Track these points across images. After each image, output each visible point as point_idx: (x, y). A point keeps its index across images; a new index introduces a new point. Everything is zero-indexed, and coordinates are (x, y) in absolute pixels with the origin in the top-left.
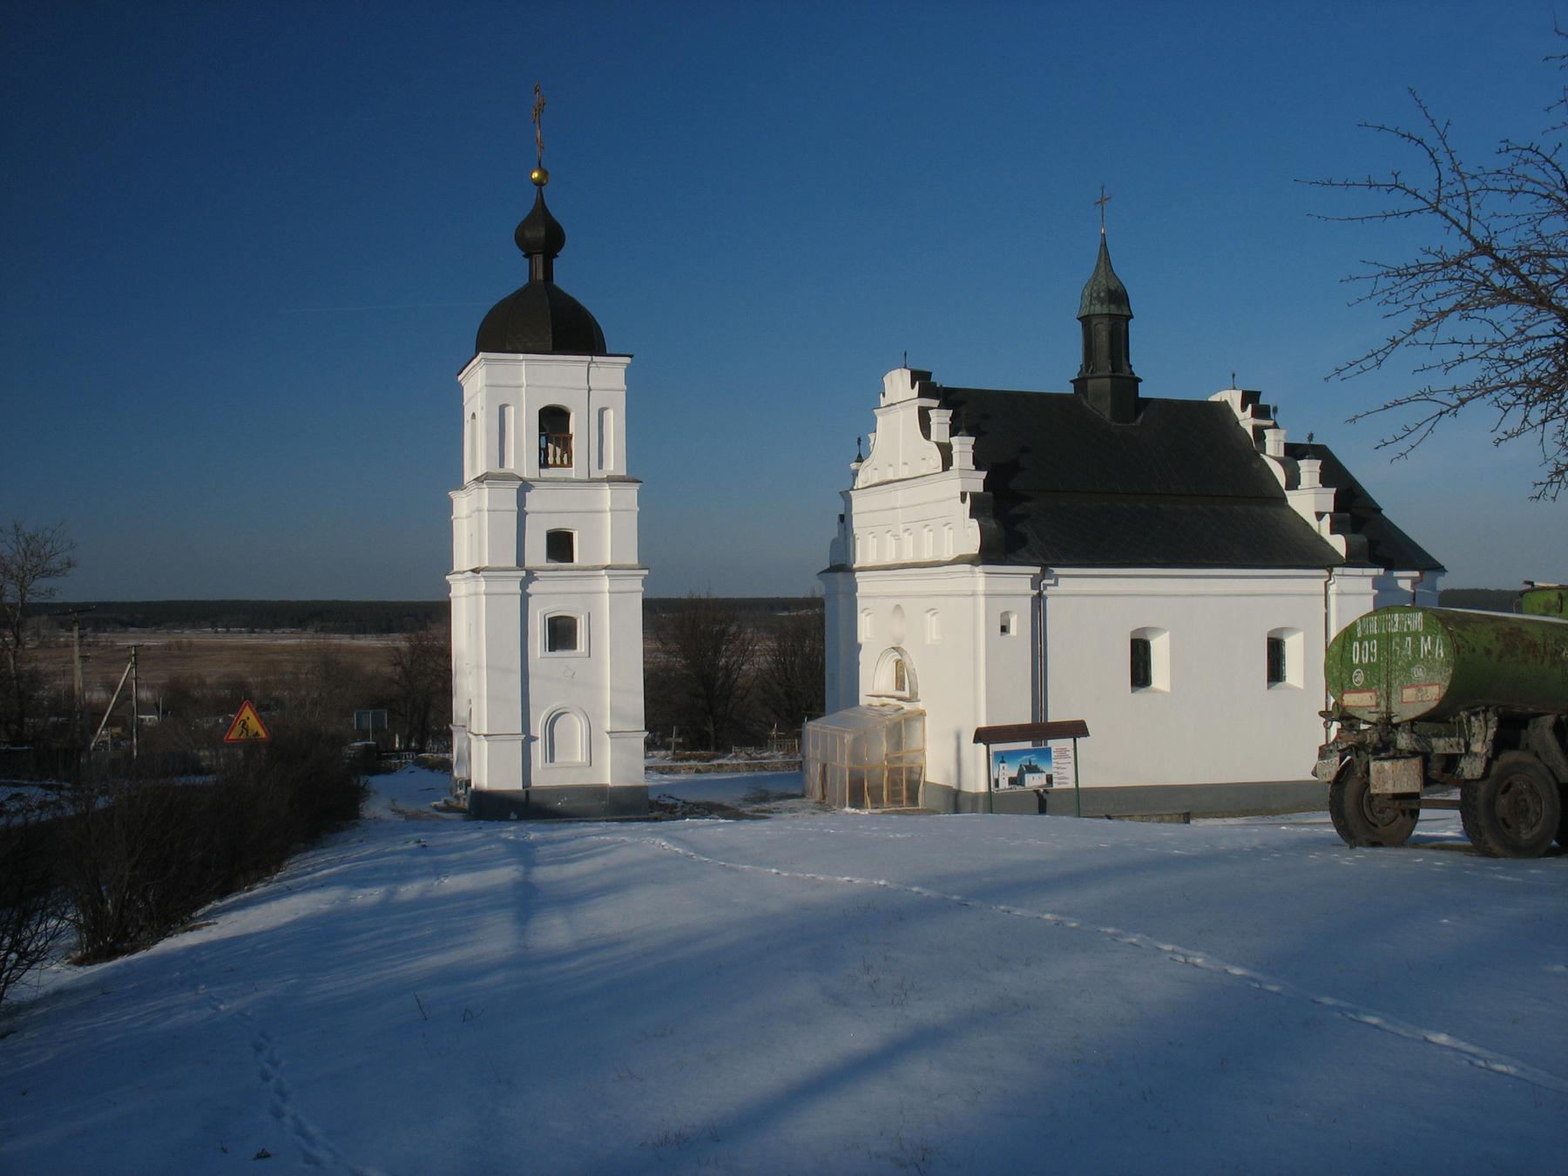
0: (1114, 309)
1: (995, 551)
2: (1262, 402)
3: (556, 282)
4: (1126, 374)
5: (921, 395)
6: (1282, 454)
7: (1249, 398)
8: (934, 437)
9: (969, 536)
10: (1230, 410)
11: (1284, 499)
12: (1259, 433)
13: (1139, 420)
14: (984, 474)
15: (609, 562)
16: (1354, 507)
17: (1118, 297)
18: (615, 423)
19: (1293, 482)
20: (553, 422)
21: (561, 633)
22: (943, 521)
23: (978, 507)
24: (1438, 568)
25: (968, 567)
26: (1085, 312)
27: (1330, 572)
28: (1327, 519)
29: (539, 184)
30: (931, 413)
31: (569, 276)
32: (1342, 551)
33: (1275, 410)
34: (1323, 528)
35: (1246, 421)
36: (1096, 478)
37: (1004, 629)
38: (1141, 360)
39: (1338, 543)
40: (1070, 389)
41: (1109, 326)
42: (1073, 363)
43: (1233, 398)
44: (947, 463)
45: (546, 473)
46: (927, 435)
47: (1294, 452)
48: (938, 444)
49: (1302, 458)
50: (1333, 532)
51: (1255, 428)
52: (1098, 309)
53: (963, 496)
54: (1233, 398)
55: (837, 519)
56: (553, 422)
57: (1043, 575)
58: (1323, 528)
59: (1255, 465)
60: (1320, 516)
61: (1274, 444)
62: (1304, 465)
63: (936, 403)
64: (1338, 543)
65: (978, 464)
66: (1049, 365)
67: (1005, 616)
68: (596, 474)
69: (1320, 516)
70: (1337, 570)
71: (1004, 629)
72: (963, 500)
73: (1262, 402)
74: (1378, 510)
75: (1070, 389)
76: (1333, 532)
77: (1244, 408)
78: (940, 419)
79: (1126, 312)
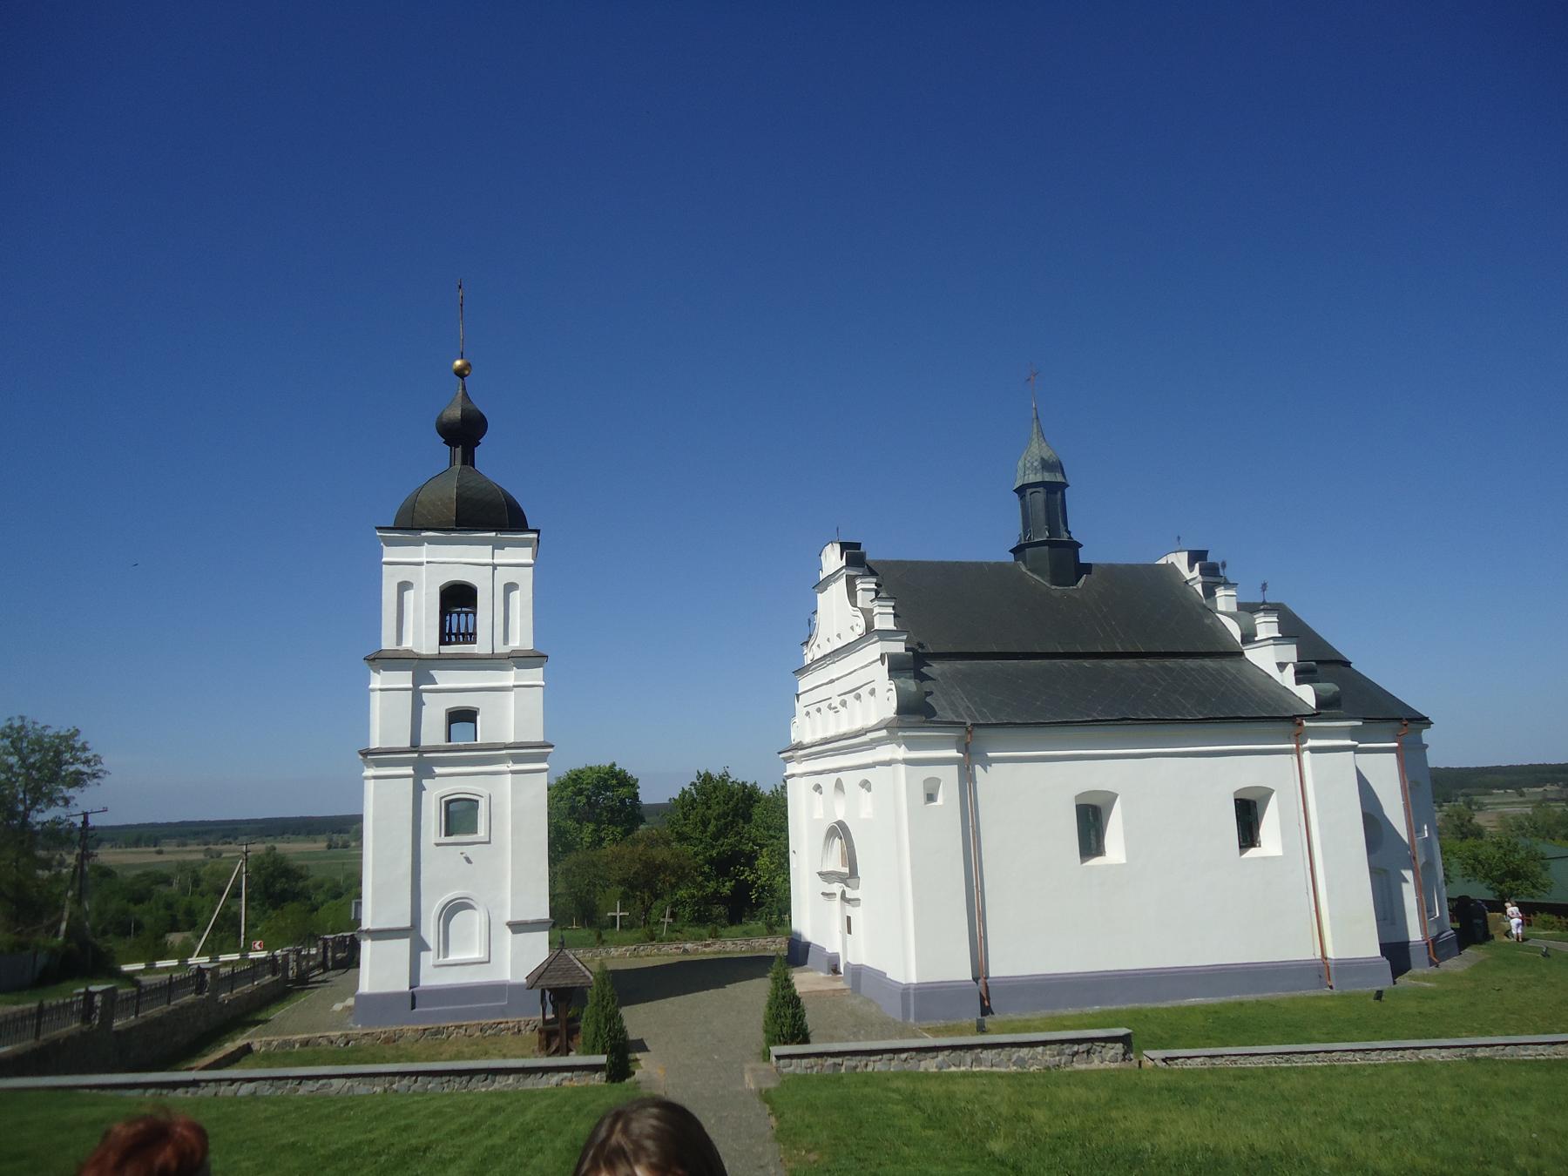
0: (1048, 477)
2: (1211, 559)
4: (1065, 538)
5: (849, 564)
6: (1234, 609)
7: (1196, 557)
10: (1177, 571)
11: (1242, 654)
12: (1209, 591)
15: (511, 739)
16: (1318, 661)
18: (521, 602)
19: (1249, 637)
20: (458, 598)
21: (460, 817)
23: (896, 667)
24: (1424, 721)
25: (884, 733)
28: (1290, 670)
29: (460, 373)
32: (1312, 702)
33: (1224, 565)
34: (1287, 679)
36: (1047, 651)
37: (931, 798)
38: (1077, 528)
41: (1048, 498)
42: (1014, 536)
43: (1180, 560)
45: (447, 649)
46: (854, 604)
47: (1248, 609)
49: (1259, 611)
50: (1298, 682)
53: (882, 656)
54: (1180, 560)
56: (458, 598)
58: (1287, 679)
59: (1208, 621)
60: (1282, 666)
61: (1225, 600)
62: (1260, 619)
64: (1307, 694)
66: (988, 536)
68: (501, 649)
69: (1282, 666)
73: (1211, 559)
74: (1347, 664)
75: (1011, 558)
76: (1298, 682)
79: (1060, 479)
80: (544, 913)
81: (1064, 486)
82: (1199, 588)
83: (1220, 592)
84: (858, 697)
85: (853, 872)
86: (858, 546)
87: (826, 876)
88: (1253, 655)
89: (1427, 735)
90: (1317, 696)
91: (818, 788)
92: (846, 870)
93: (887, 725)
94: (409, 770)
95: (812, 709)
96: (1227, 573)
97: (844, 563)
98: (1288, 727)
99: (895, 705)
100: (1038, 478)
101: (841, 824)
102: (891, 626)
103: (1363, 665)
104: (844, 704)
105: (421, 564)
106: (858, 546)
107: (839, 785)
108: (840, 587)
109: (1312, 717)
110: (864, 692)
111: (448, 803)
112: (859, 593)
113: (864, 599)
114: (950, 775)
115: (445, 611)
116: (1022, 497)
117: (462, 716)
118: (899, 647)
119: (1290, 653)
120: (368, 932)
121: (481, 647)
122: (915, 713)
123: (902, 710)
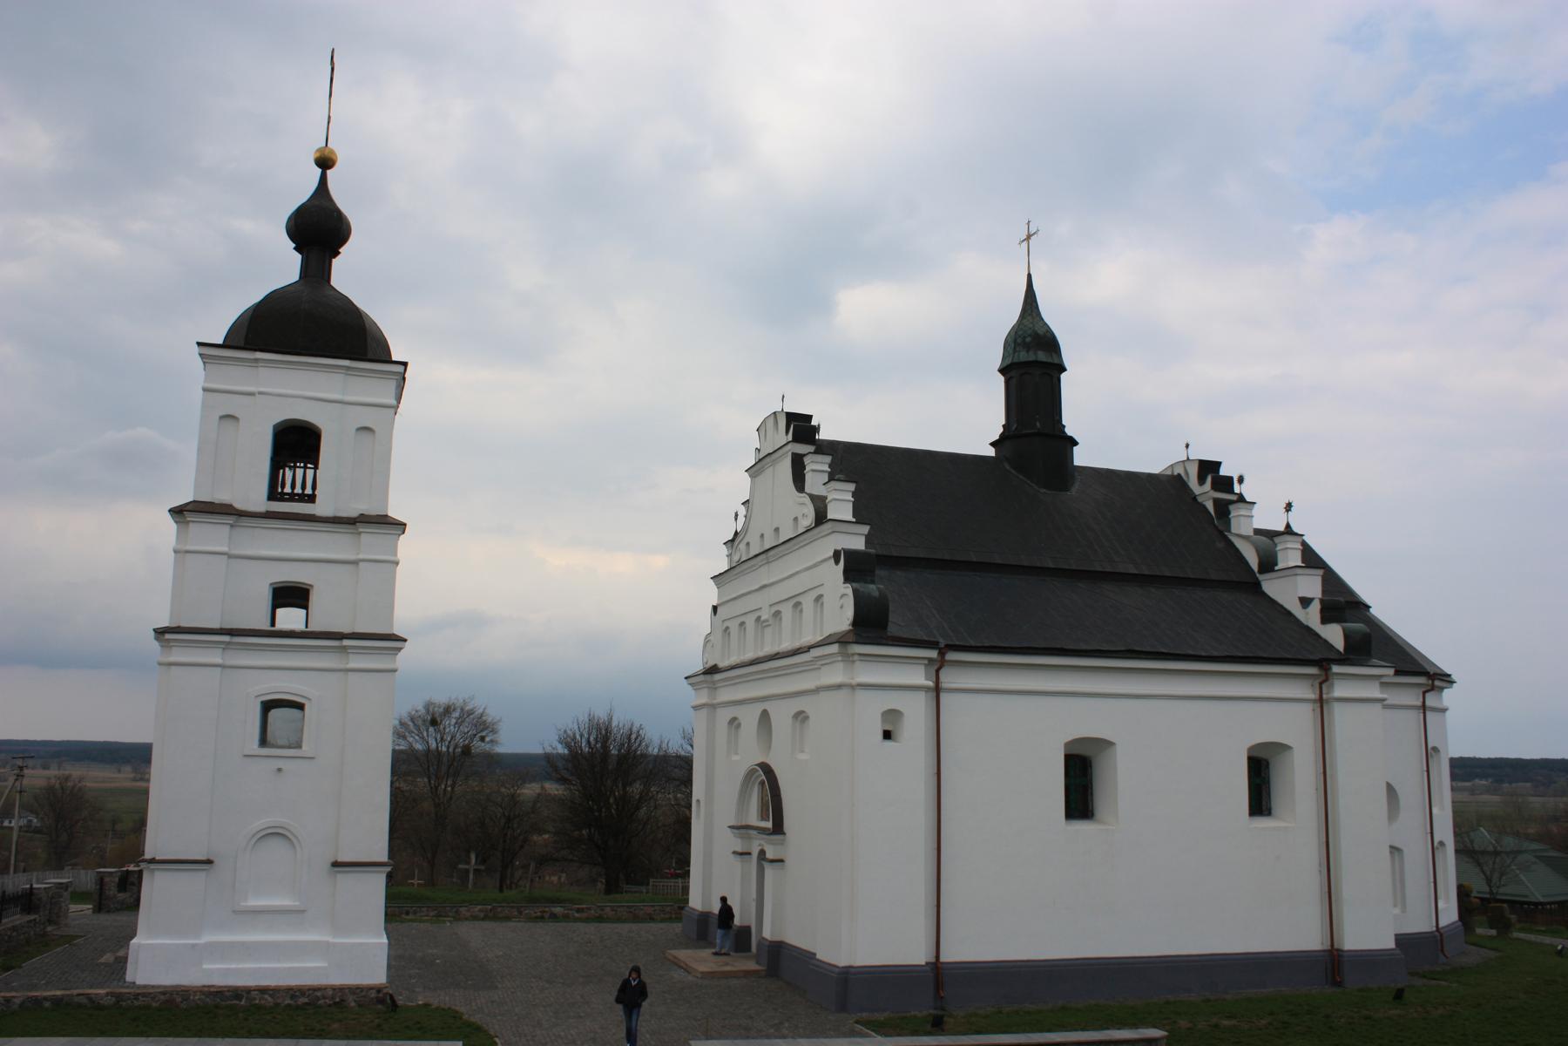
0: (1042, 356)
1: (870, 625)
2: (1223, 472)
3: (333, 283)
5: (796, 439)
8: (807, 489)
9: (838, 607)
11: (1258, 584)
12: (1223, 509)
13: (1075, 489)
14: (866, 529)
17: (1049, 343)
19: (1268, 564)
20: (296, 443)
22: (814, 594)
23: (855, 567)
25: (835, 648)
26: (1008, 362)
27: (1327, 670)
28: (1315, 607)
30: (807, 460)
31: (349, 274)
33: (1241, 480)
34: (1311, 617)
35: (1205, 493)
39: (1334, 635)
40: (991, 452)
44: (821, 518)
48: (812, 497)
50: (1325, 620)
51: (1216, 502)
52: (1024, 356)
55: (710, 609)
56: (296, 443)
57: (937, 667)
63: (811, 448)
64: (1334, 635)
65: (860, 516)
67: (892, 715)
70: (1336, 669)
71: (887, 735)
72: (837, 562)
73: (1223, 472)
75: (991, 452)
76: (1325, 620)
77: (1201, 480)
78: (818, 467)
80: (379, 849)
81: (1062, 369)
82: (1210, 506)
83: (1236, 512)
84: (798, 604)
85: (778, 828)
86: (810, 417)
87: (741, 829)
88: (1272, 587)
89: (1448, 696)
90: (1347, 637)
91: (734, 722)
92: (769, 825)
93: (842, 640)
94: (215, 657)
95: (734, 625)
96: (1246, 490)
97: (790, 437)
98: (1313, 670)
99: (849, 613)
100: (1031, 357)
101: (767, 769)
102: (850, 517)
103: (1382, 610)
104: (777, 614)
105: (252, 394)
106: (810, 417)
107: (765, 715)
108: (786, 466)
109: (1342, 661)
110: (808, 602)
111: (268, 706)
112: (809, 477)
113: (816, 480)
114: (915, 710)
115: (278, 463)
116: (1007, 383)
117: (291, 595)
118: (858, 544)
119: (1311, 585)
120: (153, 861)
121: (321, 508)
122: (870, 625)
123: (856, 622)
